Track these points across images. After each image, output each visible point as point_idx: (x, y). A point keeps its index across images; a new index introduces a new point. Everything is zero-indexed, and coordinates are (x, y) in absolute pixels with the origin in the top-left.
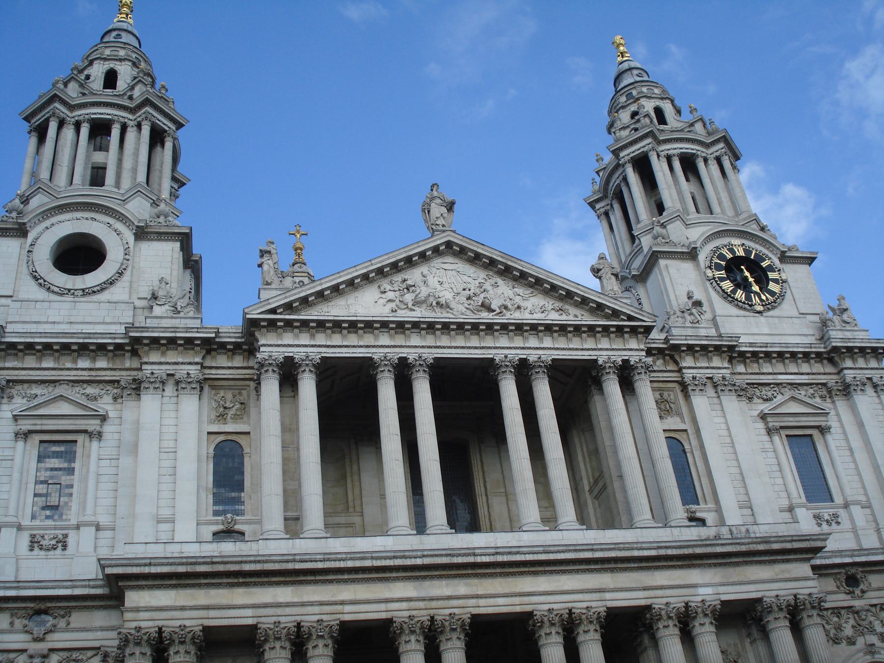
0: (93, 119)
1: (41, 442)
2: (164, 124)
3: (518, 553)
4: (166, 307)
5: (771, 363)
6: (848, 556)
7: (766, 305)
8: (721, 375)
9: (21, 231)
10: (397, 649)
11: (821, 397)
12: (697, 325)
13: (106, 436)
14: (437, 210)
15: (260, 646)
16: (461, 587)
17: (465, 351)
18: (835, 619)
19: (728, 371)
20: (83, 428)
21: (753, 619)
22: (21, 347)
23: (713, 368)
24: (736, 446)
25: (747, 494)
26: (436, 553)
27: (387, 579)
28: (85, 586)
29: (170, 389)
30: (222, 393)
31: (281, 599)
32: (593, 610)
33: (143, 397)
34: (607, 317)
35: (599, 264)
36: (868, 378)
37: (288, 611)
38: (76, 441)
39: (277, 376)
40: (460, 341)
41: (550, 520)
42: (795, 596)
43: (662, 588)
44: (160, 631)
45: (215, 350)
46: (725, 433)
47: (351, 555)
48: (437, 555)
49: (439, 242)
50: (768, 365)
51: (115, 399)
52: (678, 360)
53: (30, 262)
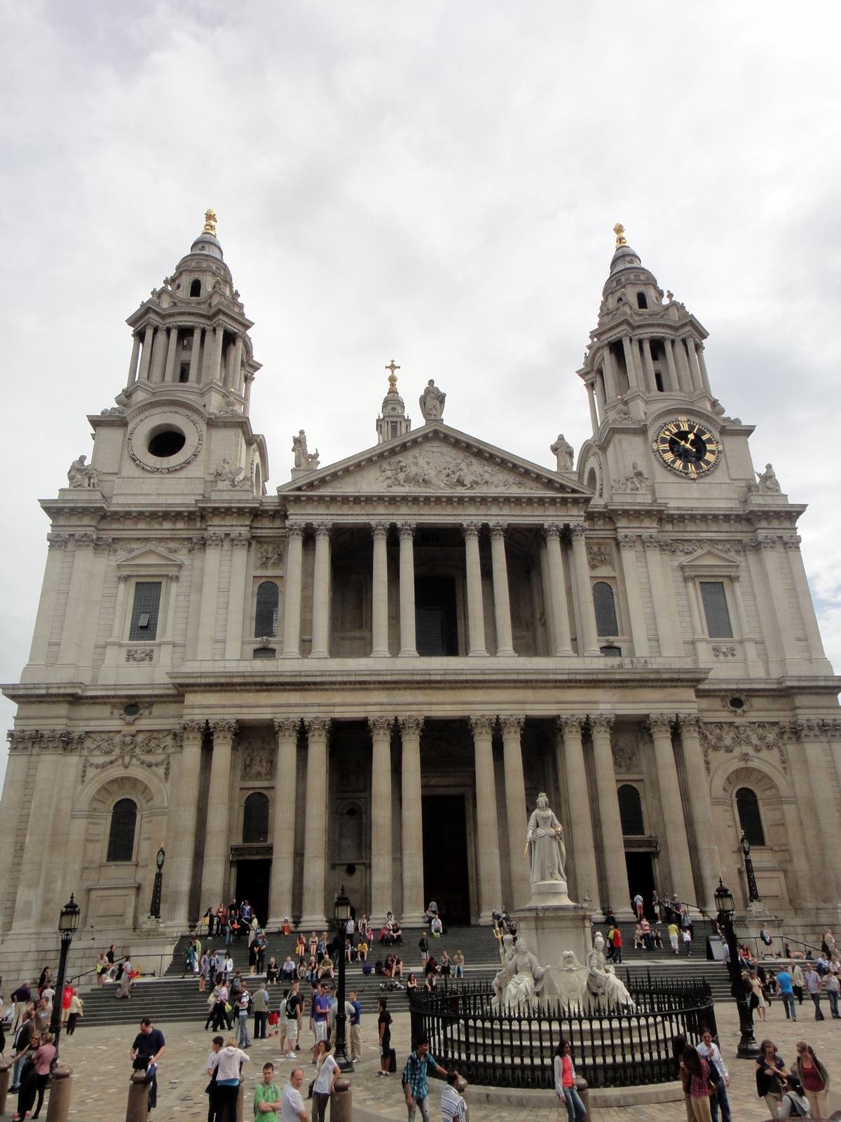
1: (137, 583)
3: (460, 674)
4: (227, 482)
5: (695, 522)
6: (734, 684)
9: (123, 423)
10: (370, 739)
11: (736, 551)
13: (181, 579)
16: (420, 696)
18: (718, 731)
19: (656, 530)
20: (165, 573)
21: (645, 728)
22: (122, 514)
23: (643, 528)
24: (653, 591)
25: (656, 630)
27: (367, 689)
28: (161, 688)
29: (227, 544)
30: (265, 546)
31: (291, 701)
35: (556, 443)
36: (778, 537)
37: (296, 709)
38: (161, 583)
40: (438, 510)
42: (677, 715)
43: (570, 703)
45: (261, 515)
47: (341, 673)
48: (403, 674)
51: (190, 551)
53: (130, 447)
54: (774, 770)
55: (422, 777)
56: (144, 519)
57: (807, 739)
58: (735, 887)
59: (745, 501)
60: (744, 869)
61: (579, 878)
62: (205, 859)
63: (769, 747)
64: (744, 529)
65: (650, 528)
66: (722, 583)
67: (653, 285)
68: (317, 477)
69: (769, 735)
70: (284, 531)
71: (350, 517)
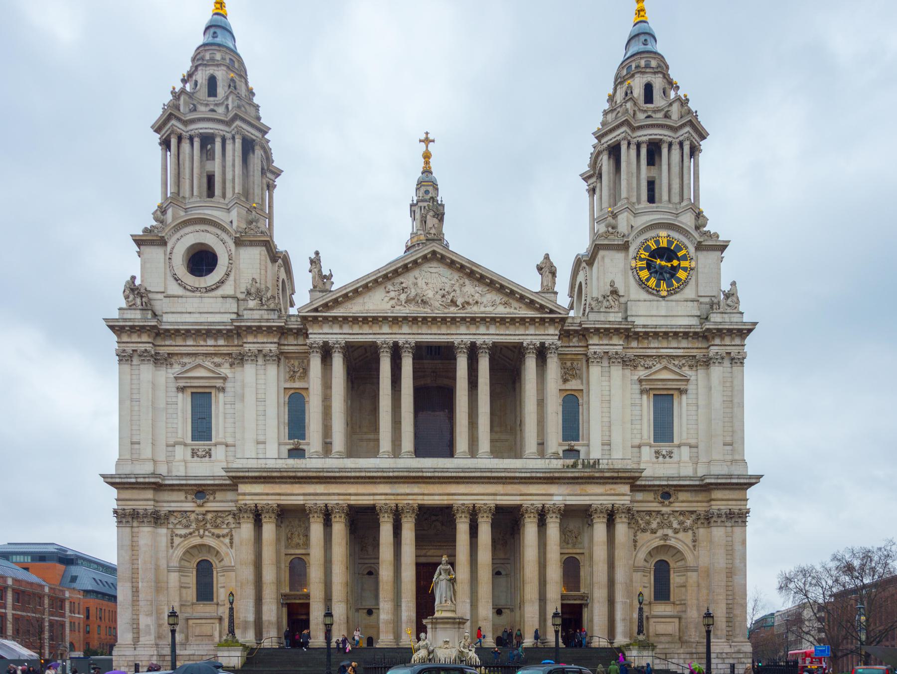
0: (201, 133)
2: (252, 134)
5: (658, 339)
7: (670, 290)
8: (615, 351)
12: (610, 310)
15: (308, 515)
16: (416, 489)
19: (621, 347)
22: (172, 332)
23: (611, 345)
24: (612, 402)
25: (610, 436)
26: (401, 470)
27: (375, 483)
29: (260, 361)
31: (318, 491)
32: (488, 506)
33: (245, 366)
36: (727, 353)
37: (321, 497)
41: (473, 452)
42: (613, 505)
44: (256, 506)
45: (286, 333)
46: (607, 393)
48: (401, 471)
50: (656, 341)
53: (171, 267)
55: (416, 549)
56: (191, 336)
59: (707, 318)
61: (526, 620)
62: (263, 601)
64: (700, 346)
65: (616, 345)
67: (661, 72)
70: (307, 347)
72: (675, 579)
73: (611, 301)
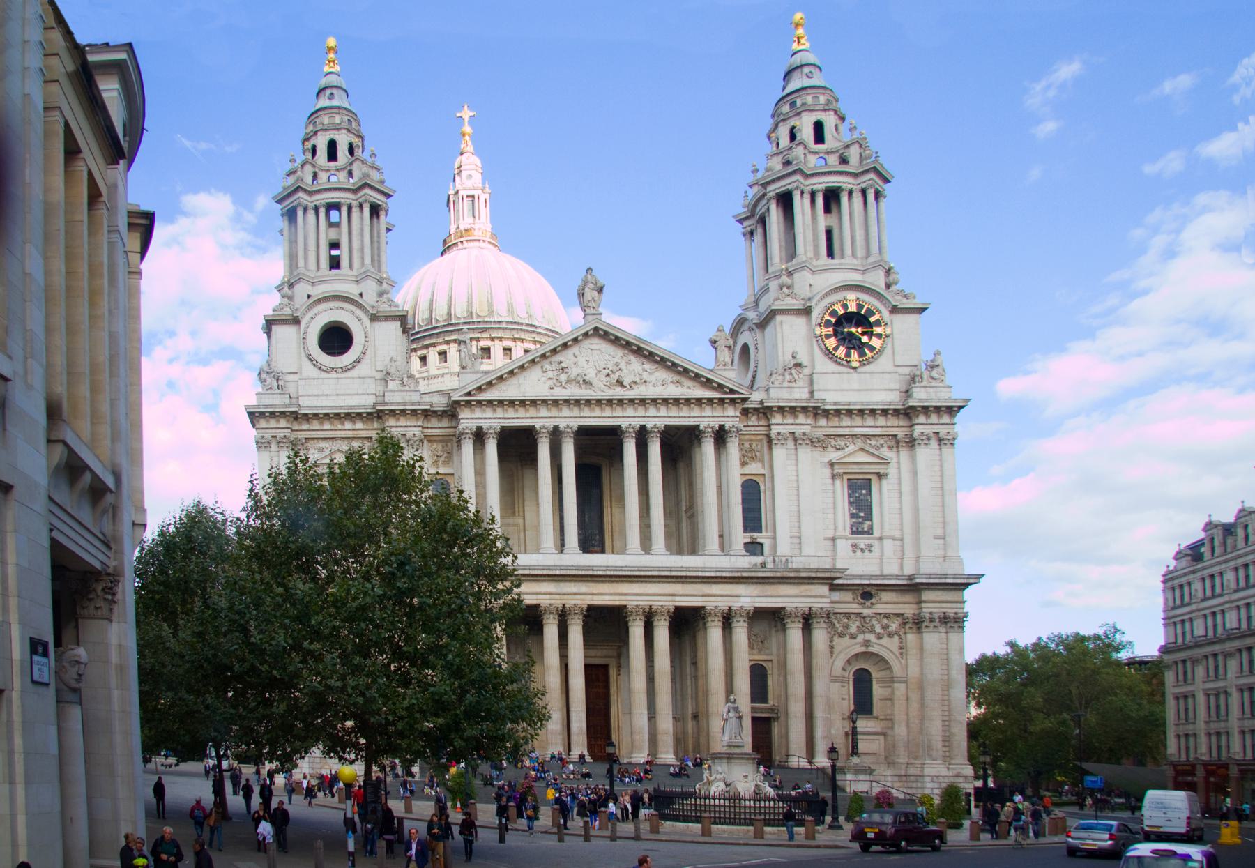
3: (621, 570)
10: (542, 621)
11: (889, 447)
12: (794, 385)
14: (590, 294)
16: (583, 588)
17: (601, 420)
19: (809, 427)
25: (799, 527)
34: (714, 389)
35: (717, 336)
39: (472, 441)
40: (597, 412)
43: (715, 596)
49: (588, 329)
52: (769, 416)
54: (893, 656)
57: (927, 630)
58: (842, 746)
60: (850, 732)
63: (890, 635)
64: (901, 423)
65: (803, 424)
66: (870, 480)
68: (485, 381)
69: (892, 625)
71: (516, 421)
72: (878, 691)
73: (795, 375)
